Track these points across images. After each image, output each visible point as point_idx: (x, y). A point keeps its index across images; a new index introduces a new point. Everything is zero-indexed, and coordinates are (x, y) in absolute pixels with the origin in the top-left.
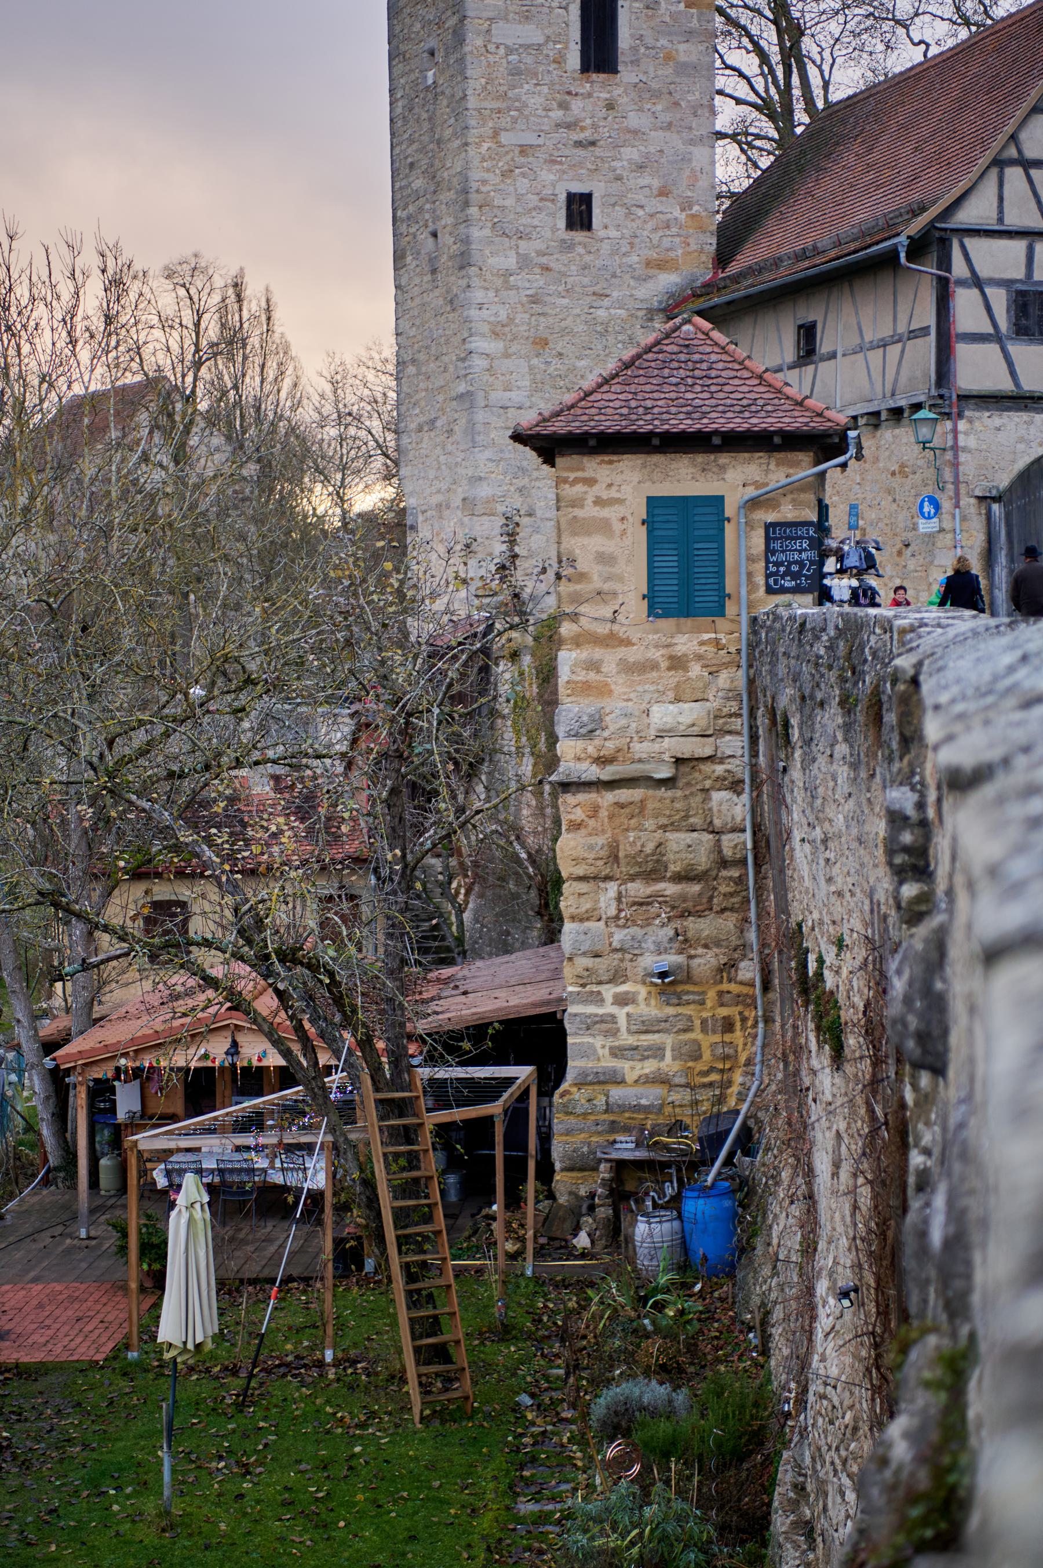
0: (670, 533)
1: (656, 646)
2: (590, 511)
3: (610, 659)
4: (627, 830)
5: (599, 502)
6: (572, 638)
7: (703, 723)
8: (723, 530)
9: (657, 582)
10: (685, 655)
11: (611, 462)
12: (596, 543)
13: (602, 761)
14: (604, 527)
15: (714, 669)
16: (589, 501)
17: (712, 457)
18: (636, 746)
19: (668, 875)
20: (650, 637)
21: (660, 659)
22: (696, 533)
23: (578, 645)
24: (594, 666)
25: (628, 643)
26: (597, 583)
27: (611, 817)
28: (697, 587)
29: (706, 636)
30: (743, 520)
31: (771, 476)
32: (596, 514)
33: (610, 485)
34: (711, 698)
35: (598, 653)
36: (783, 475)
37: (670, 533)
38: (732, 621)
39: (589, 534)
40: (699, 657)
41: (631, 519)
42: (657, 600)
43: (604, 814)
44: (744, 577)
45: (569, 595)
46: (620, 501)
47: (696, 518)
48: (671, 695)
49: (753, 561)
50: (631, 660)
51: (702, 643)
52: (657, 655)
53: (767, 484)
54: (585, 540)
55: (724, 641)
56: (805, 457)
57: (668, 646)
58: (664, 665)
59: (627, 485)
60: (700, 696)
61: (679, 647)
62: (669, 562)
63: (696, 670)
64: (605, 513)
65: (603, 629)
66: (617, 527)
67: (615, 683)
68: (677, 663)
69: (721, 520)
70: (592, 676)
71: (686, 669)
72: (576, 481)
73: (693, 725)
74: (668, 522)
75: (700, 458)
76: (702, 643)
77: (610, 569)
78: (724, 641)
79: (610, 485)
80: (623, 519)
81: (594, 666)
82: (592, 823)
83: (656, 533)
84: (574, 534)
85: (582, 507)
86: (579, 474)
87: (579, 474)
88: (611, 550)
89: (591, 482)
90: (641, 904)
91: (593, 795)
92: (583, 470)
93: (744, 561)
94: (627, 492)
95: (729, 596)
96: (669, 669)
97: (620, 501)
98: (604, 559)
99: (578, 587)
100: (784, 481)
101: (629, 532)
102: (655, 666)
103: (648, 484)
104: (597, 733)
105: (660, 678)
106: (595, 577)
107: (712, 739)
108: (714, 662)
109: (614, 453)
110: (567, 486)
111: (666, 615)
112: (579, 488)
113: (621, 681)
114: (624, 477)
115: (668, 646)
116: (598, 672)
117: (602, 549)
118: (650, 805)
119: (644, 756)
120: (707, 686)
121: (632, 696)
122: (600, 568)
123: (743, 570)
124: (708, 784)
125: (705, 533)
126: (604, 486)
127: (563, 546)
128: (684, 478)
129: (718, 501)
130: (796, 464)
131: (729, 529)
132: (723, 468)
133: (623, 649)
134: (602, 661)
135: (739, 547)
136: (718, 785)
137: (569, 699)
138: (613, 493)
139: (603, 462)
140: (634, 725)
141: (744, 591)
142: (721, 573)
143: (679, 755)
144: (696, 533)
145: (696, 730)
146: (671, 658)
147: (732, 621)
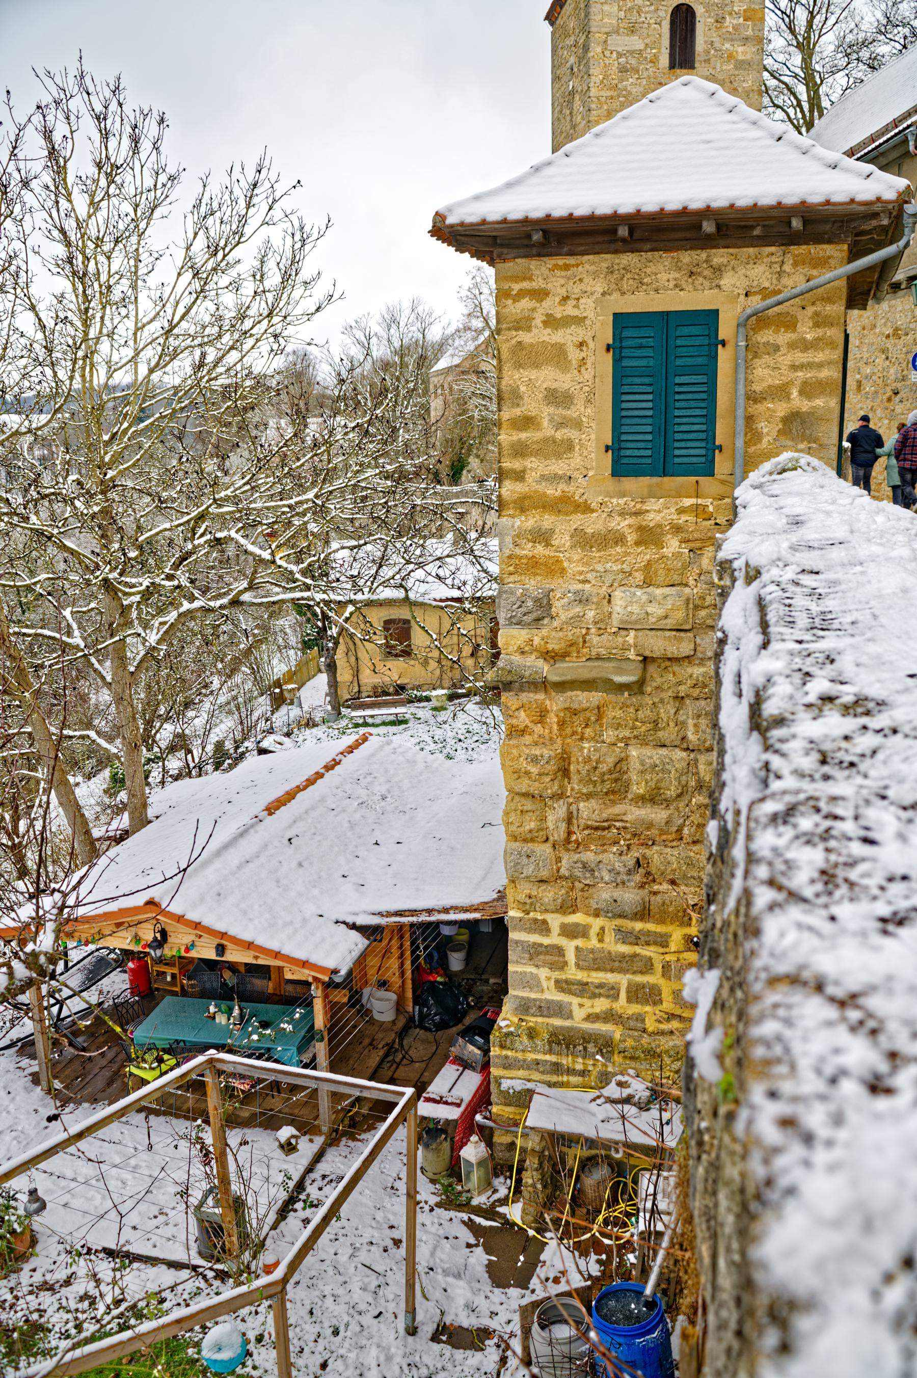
0: (643, 362)
1: (622, 514)
2: (539, 335)
3: (563, 528)
4: (582, 739)
5: (551, 322)
6: (515, 502)
7: (680, 615)
8: (716, 357)
9: (625, 429)
10: (659, 526)
11: (567, 267)
12: (548, 377)
13: (551, 656)
14: (558, 357)
15: (698, 544)
16: (539, 319)
17: (704, 255)
18: (594, 639)
19: (630, 796)
20: (614, 501)
21: (627, 531)
22: (679, 362)
23: (523, 510)
24: (542, 537)
25: (587, 509)
26: (547, 430)
27: (562, 724)
28: (678, 436)
29: (688, 502)
30: (743, 343)
31: (785, 281)
32: (547, 339)
33: (565, 299)
34: (691, 582)
35: (548, 521)
36: (803, 279)
37: (643, 362)
38: (723, 482)
39: (537, 366)
40: (677, 529)
41: (591, 345)
42: (623, 453)
43: (552, 719)
44: (741, 422)
45: (512, 446)
46: (579, 321)
47: (679, 342)
48: (639, 577)
49: (755, 401)
50: (590, 531)
51: (681, 511)
52: (623, 524)
53: (780, 292)
54: (533, 374)
55: (711, 509)
56: (836, 251)
57: (637, 514)
58: (631, 538)
59: (590, 296)
60: (676, 578)
61: (651, 515)
62: (642, 404)
63: (672, 545)
64: (559, 337)
65: (553, 491)
66: (574, 355)
67: (569, 560)
68: (649, 536)
69: (714, 343)
70: (540, 550)
71: (660, 544)
72: (522, 294)
73: (666, 617)
74: (641, 347)
75: (687, 257)
76: (681, 511)
77: (565, 412)
78: (711, 509)
79: (565, 299)
80: (581, 344)
81: (542, 537)
82: (538, 729)
83: (625, 363)
84: (518, 366)
85: (529, 329)
86: (526, 285)
87: (526, 285)
88: (566, 386)
89: (540, 295)
90: (597, 829)
91: (540, 696)
92: (530, 279)
93: (741, 401)
94: (588, 307)
95: (720, 448)
96: (637, 543)
97: (579, 321)
98: (556, 397)
99: (523, 435)
100: (802, 286)
101: (589, 362)
102: (620, 539)
103: (616, 295)
104: (546, 621)
105: (627, 554)
106: (545, 423)
107: (690, 635)
108: (696, 535)
109: (571, 254)
110: (510, 302)
111: (636, 471)
112: (526, 303)
113: (576, 557)
114: (583, 286)
115: (637, 514)
116: (548, 544)
117: (555, 385)
118: (612, 713)
119: (603, 651)
120: (686, 567)
121: (590, 576)
122: (552, 410)
123: (740, 412)
124: (683, 690)
125: (690, 361)
126: (557, 300)
127: (504, 383)
128: (664, 285)
129: (714, 314)
130: (822, 263)
131: (724, 356)
132: (718, 271)
133: (579, 516)
134: (552, 531)
135: (736, 382)
136: (696, 692)
137: (512, 578)
138: (570, 310)
139: (556, 266)
140: (591, 614)
141: (740, 442)
142: (710, 418)
143: (647, 653)
144: (679, 362)
145: (670, 623)
146: (641, 529)
147: (723, 482)
